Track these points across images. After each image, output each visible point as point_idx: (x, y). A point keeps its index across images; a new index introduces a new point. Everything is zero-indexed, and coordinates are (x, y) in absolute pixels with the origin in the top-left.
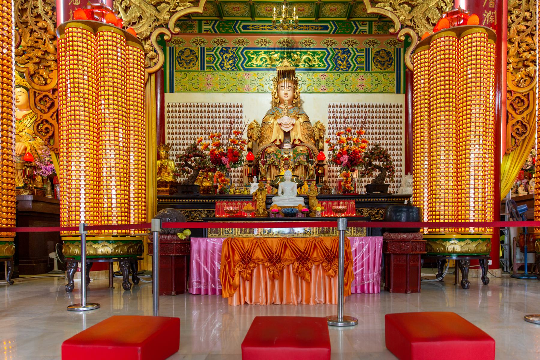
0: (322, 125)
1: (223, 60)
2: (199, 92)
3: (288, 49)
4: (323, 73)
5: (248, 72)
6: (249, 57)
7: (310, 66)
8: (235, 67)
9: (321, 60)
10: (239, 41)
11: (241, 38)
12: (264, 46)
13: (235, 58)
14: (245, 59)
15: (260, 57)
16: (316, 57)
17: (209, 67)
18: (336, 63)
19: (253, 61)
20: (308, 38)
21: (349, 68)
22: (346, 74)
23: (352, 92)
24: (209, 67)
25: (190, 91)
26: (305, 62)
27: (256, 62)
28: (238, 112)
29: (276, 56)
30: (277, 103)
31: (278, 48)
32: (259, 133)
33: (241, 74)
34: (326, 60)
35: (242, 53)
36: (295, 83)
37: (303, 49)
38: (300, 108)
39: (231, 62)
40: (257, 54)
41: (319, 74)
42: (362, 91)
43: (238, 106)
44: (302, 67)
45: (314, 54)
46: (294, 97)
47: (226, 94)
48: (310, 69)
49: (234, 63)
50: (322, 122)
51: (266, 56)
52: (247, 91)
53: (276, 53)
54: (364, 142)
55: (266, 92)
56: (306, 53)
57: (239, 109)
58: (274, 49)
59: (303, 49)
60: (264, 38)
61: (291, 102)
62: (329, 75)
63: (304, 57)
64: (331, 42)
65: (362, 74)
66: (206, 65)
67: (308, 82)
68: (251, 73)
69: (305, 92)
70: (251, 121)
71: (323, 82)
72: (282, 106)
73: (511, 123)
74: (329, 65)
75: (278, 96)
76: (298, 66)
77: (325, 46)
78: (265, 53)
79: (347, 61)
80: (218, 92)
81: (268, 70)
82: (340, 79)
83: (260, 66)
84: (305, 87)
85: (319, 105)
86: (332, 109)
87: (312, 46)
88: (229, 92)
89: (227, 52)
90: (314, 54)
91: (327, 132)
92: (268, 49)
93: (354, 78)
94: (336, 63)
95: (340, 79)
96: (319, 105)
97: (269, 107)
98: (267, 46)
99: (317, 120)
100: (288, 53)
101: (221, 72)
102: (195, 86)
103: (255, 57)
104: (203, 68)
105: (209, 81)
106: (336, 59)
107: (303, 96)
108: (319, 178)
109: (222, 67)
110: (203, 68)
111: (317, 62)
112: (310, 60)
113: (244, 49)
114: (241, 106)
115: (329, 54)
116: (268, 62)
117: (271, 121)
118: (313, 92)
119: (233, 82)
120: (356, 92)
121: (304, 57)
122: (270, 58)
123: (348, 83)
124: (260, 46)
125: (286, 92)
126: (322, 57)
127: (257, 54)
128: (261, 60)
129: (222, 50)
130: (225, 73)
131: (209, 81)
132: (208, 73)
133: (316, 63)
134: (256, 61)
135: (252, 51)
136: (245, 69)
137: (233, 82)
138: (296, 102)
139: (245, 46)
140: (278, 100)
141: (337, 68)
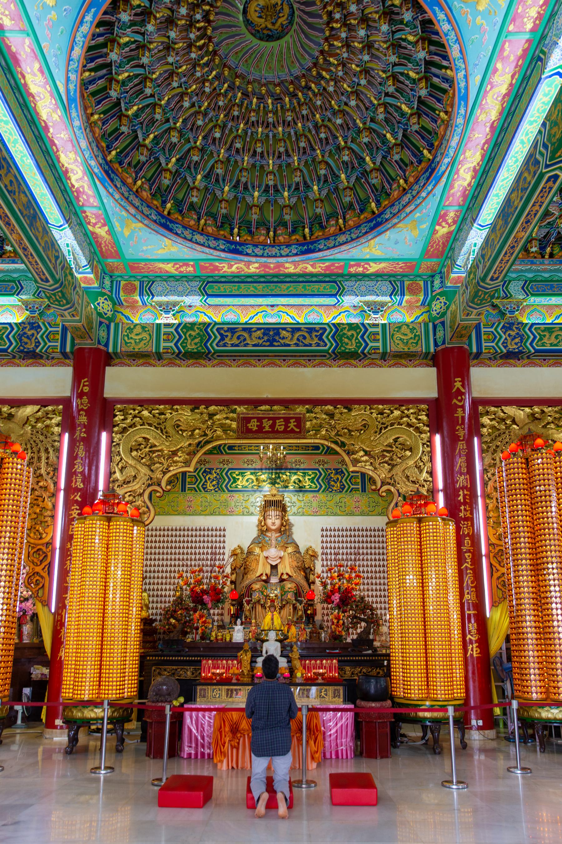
0: (313, 551)
1: (206, 481)
2: (179, 514)
3: (276, 469)
4: (315, 494)
5: (232, 494)
6: (234, 478)
7: (300, 487)
8: (218, 488)
9: (312, 480)
10: (224, 461)
11: (226, 457)
12: (250, 466)
13: (219, 479)
14: (230, 480)
15: (246, 478)
16: (307, 478)
17: (190, 489)
18: (329, 484)
19: (239, 482)
20: (298, 458)
21: (343, 489)
22: (339, 495)
23: (347, 515)
24: (190, 489)
25: (168, 514)
26: (295, 482)
27: (241, 483)
28: (220, 536)
29: (264, 477)
30: (263, 530)
31: (266, 469)
32: (243, 562)
33: (225, 496)
34: (317, 480)
35: (226, 474)
36: (284, 509)
37: (293, 469)
38: (290, 535)
39: (214, 483)
40: (242, 474)
41: (310, 495)
42: (357, 513)
43: (220, 530)
44: (291, 488)
45: (305, 474)
46: (282, 525)
47: (208, 517)
48: (301, 490)
49: (218, 484)
50: (314, 547)
51: (253, 477)
52: (231, 513)
53: (264, 474)
54: (359, 577)
55: (252, 514)
56: (295, 474)
57: (222, 533)
58: (262, 469)
59: (293, 469)
60: (250, 457)
61: (279, 530)
62: (321, 496)
63: (294, 478)
64: (323, 461)
65: (357, 495)
66: (187, 486)
67: (298, 504)
68: (236, 495)
69: (294, 514)
70: (235, 546)
71: (315, 504)
72: (269, 534)
73: (496, 575)
74: (321, 486)
75: (265, 524)
76: (287, 487)
77: (317, 466)
78: (252, 474)
79: (341, 482)
80: (200, 514)
81: (255, 491)
82: (334, 501)
83: (246, 487)
84: (294, 510)
85: (310, 529)
86: (325, 533)
87: (302, 466)
88: (212, 514)
89: (210, 473)
90: (305, 474)
91: (320, 558)
92: (255, 469)
93: (349, 500)
94: (329, 484)
95: (334, 501)
96: (310, 529)
97: (254, 533)
98: (254, 466)
99: (308, 544)
100: (276, 473)
101: (203, 494)
102: (174, 509)
103: (241, 478)
104: (184, 489)
105: (189, 504)
106: (328, 479)
107: (292, 519)
108: (310, 618)
109: (204, 489)
110: (184, 489)
111: (308, 483)
112: (300, 481)
113: (230, 469)
114: (224, 530)
115: (321, 474)
116: (255, 483)
117: (257, 550)
118: (303, 515)
119: (216, 504)
120: (351, 514)
121: (294, 478)
122: (257, 479)
123: (343, 504)
124: (246, 466)
125: (273, 521)
126: (313, 478)
127: (242, 474)
128: (247, 481)
129: (205, 471)
130: (208, 496)
131: (189, 504)
132: (189, 495)
133: (307, 484)
134: (242, 482)
135: (237, 472)
136: (229, 491)
137: (216, 504)
138: (285, 529)
139: (230, 466)
140: (264, 528)
141: (329, 488)
